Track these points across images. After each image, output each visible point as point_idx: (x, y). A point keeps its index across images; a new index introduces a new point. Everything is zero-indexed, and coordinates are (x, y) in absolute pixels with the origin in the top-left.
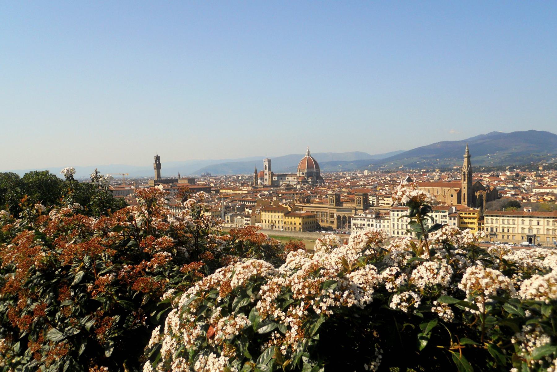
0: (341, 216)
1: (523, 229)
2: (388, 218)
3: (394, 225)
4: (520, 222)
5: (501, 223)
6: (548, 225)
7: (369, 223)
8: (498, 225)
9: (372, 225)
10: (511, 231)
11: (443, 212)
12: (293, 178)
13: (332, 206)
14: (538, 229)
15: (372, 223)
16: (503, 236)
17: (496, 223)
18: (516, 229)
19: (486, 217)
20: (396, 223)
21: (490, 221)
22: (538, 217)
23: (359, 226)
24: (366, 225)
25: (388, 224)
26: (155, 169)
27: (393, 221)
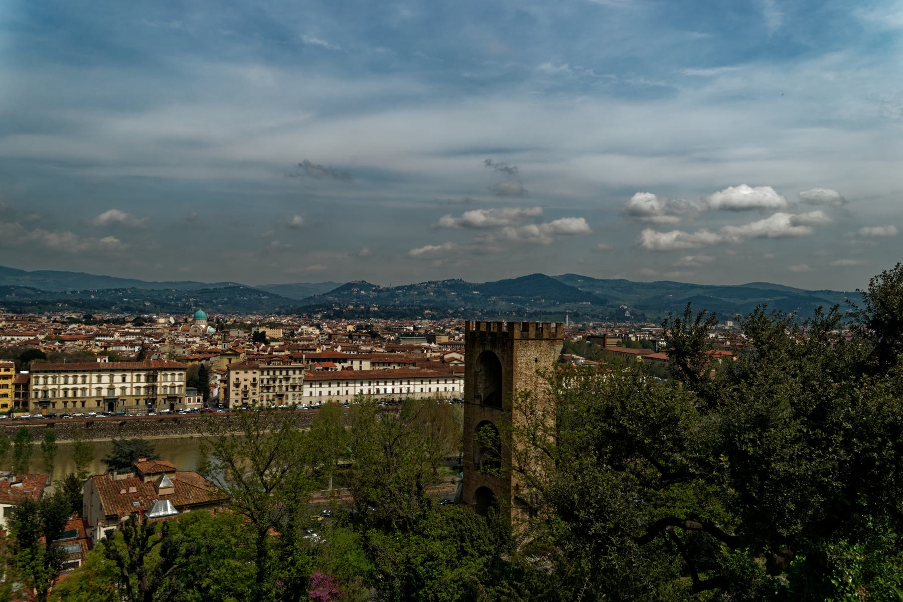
1: (99, 389)
4: (94, 379)
6: (138, 381)
8: (56, 387)
10: (79, 393)
14: (123, 389)
16: (65, 403)
17: (54, 383)
18: (88, 391)
21: (41, 381)
22: (124, 370)
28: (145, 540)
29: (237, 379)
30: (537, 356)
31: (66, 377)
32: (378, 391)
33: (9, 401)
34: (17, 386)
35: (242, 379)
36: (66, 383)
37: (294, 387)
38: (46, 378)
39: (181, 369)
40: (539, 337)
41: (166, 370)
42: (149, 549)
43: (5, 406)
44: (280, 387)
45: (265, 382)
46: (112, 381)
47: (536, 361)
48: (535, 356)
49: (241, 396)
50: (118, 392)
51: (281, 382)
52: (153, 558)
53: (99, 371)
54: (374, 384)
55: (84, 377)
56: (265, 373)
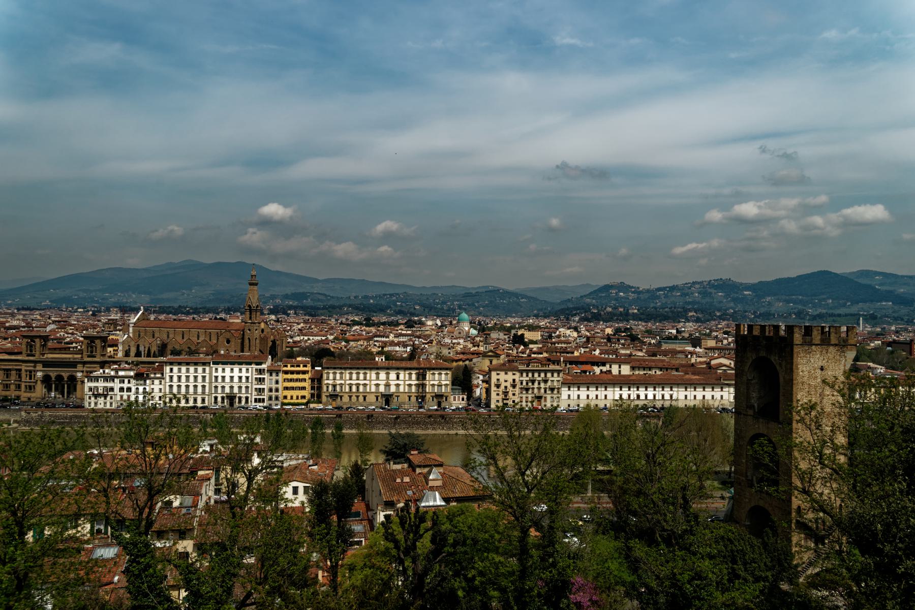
0: (53, 375)
1: (377, 385)
3: (171, 386)
4: (374, 376)
5: (348, 378)
6: (410, 379)
7: (122, 385)
8: (343, 382)
9: (129, 389)
10: (361, 389)
11: (257, 364)
13: (31, 358)
14: (398, 385)
15: (129, 385)
16: (350, 397)
17: (341, 378)
20: (175, 385)
21: (331, 376)
22: (398, 369)
23: (101, 391)
24: (116, 390)
25: (161, 387)
27: (171, 380)
28: (418, 527)
29: (498, 380)
30: (824, 363)
31: (351, 374)
32: (638, 396)
33: (306, 393)
34: (312, 380)
35: (502, 380)
36: (351, 379)
37: (552, 390)
38: (335, 373)
39: (447, 369)
40: (825, 342)
41: (434, 369)
42: (421, 536)
43: (303, 397)
44: (539, 389)
45: (524, 383)
46: (388, 378)
47: (822, 369)
48: (820, 364)
49: (501, 396)
50: (393, 389)
51: (539, 384)
52: (425, 544)
53: (378, 369)
54: (633, 389)
55: (365, 374)
56: (525, 374)
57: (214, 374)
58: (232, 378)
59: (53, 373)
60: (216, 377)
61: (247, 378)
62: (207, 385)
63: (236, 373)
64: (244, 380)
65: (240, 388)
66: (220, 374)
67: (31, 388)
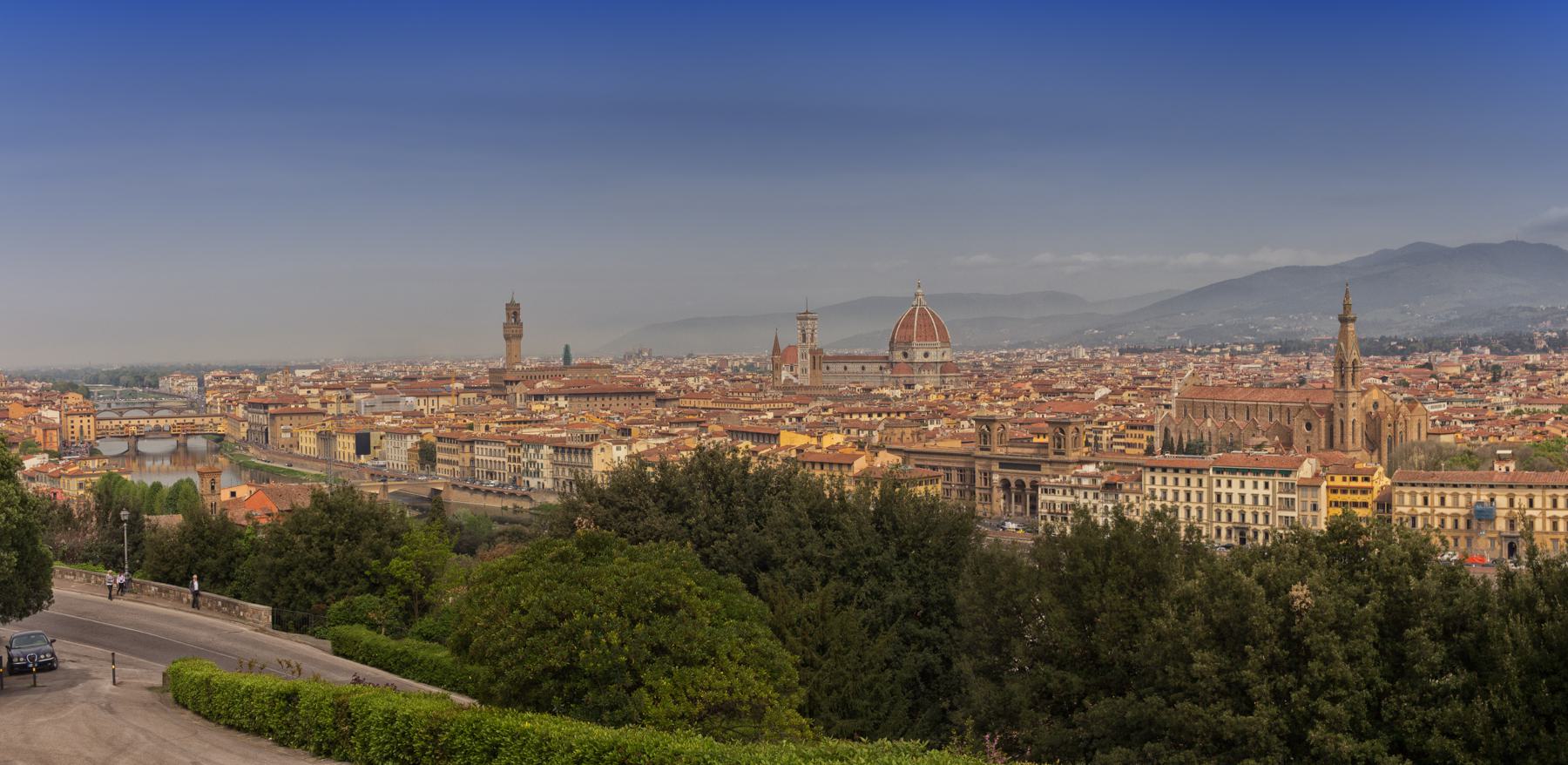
0: (1012, 480)
2: (1136, 487)
8: (1428, 510)
12: (876, 367)
13: (986, 453)
19: (1398, 489)
21: (1407, 499)
26: (507, 338)
57: (1216, 489)
58: (1243, 497)
59: (1013, 476)
60: (1219, 496)
61: (1267, 498)
62: (1204, 506)
63: (1249, 490)
64: (1261, 501)
65: (1256, 515)
66: (1224, 489)
67: (988, 498)
